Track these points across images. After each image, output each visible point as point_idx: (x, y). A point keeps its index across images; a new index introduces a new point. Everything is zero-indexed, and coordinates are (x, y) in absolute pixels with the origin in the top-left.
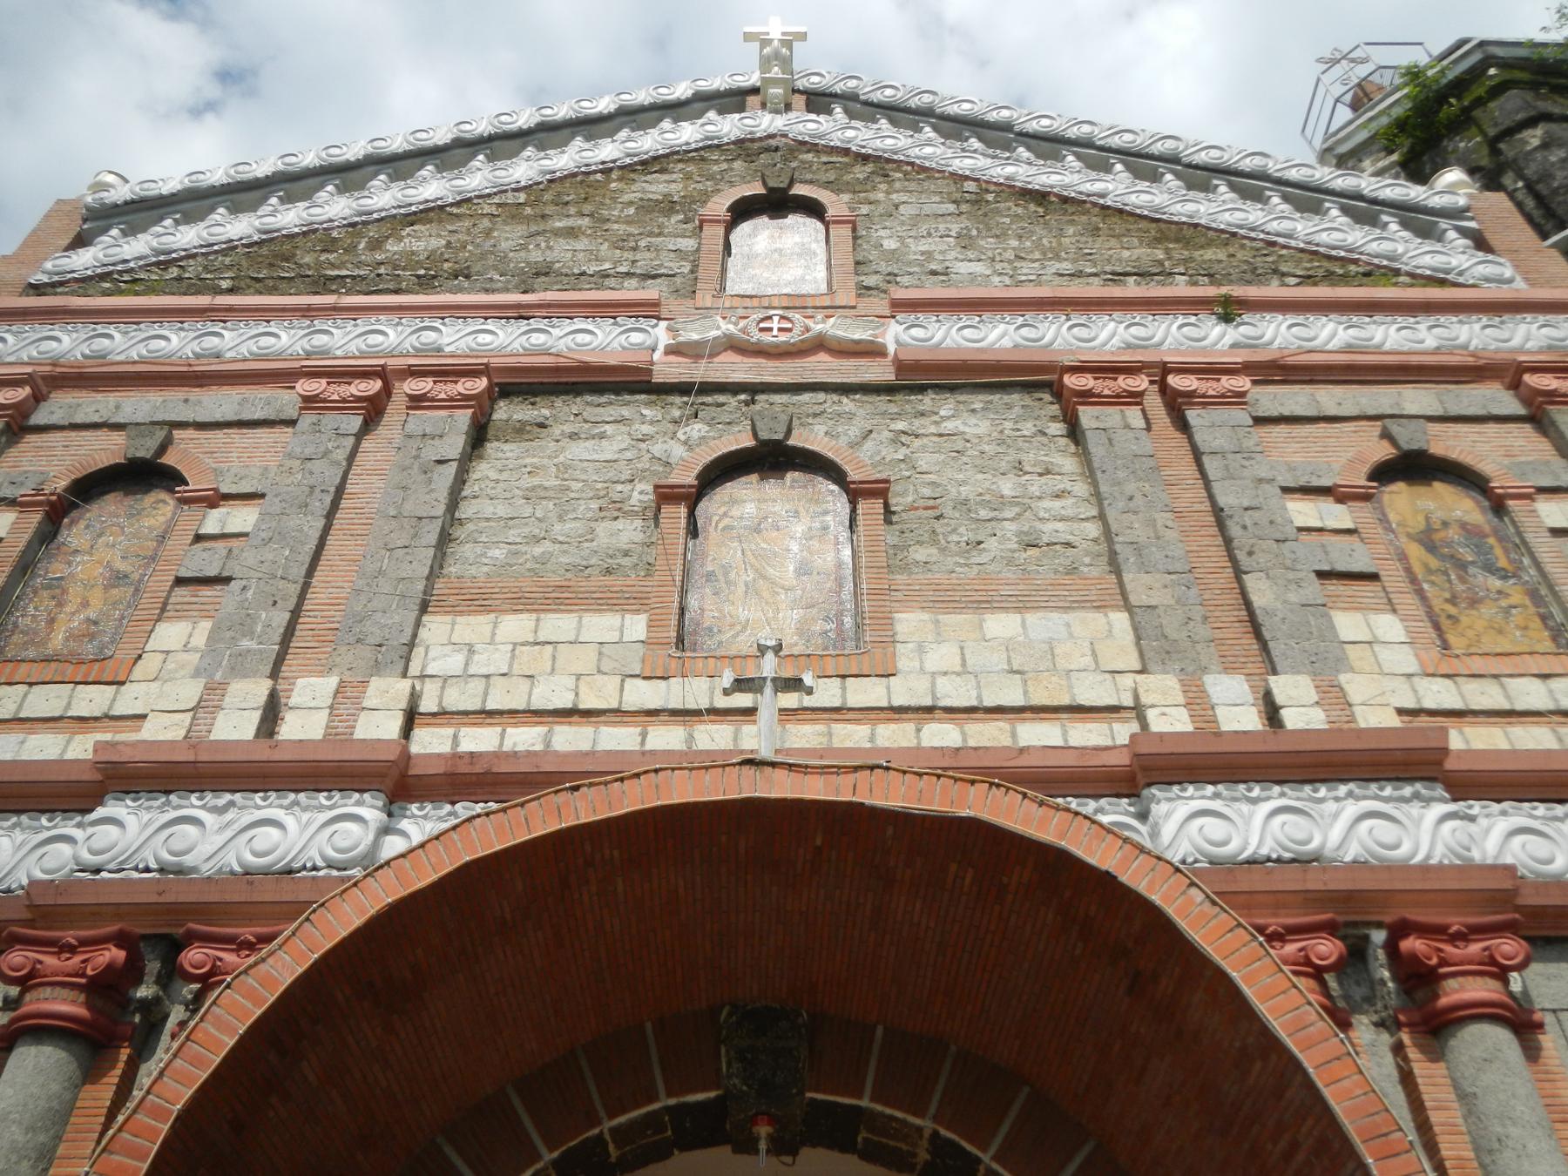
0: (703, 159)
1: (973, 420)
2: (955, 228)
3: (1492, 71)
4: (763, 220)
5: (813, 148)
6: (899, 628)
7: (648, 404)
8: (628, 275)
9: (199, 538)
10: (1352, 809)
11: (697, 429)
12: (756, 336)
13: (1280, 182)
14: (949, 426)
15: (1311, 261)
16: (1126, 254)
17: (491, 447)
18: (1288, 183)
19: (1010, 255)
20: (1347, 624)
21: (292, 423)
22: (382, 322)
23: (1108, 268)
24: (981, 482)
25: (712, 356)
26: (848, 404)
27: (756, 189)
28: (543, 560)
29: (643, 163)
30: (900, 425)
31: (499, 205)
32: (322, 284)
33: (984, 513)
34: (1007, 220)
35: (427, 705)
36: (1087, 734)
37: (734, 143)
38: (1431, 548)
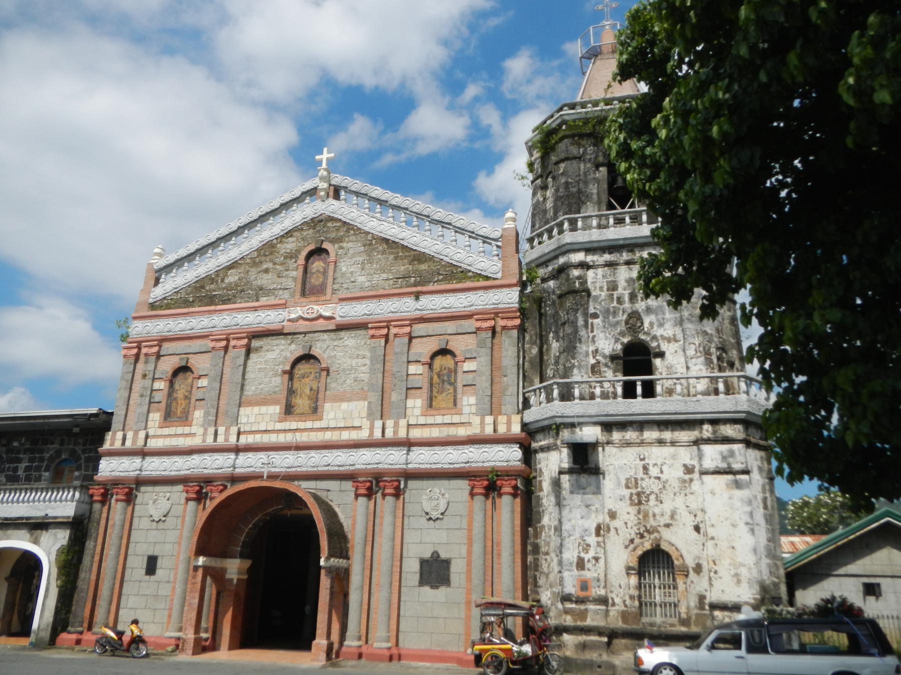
0: (302, 229)
1: (351, 340)
2: (361, 259)
3: (564, 127)
4: (316, 256)
5: (331, 219)
6: (325, 408)
7: (283, 338)
8: (281, 288)
9: (198, 388)
11: (293, 346)
12: (306, 316)
15: (449, 267)
16: (402, 268)
17: (252, 355)
19: (372, 272)
21: (210, 352)
22: (225, 315)
23: (396, 276)
24: (349, 361)
25: (297, 321)
26: (325, 336)
27: (312, 247)
28: (262, 389)
29: (286, 233)
30: (336, 343)
31: (251, 258)
32: (211, 300)
33: (348, 372)
34: (376, 254)
35: (242, 430)
37: (311, 219)
38: (439, 376)
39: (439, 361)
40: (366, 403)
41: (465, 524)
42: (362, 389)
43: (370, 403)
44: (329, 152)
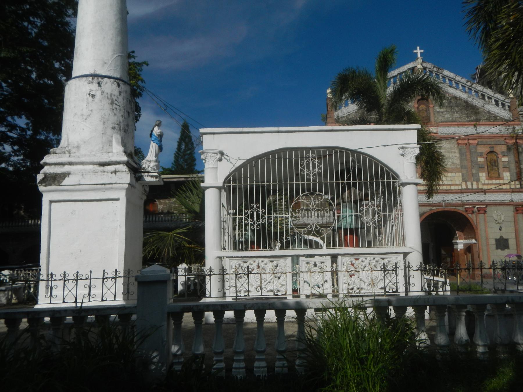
1: (447, 145)
10: (477, 196)
13: (488, 94)
14: (445, 146)
18: (489, 95)
20: (481, 174)
36: (457, 187)
39: (490, 156)
40: (460, 174)
41: (513, 224)
42: (456, 167)
43: (463, 175)
44: (420, 49)
